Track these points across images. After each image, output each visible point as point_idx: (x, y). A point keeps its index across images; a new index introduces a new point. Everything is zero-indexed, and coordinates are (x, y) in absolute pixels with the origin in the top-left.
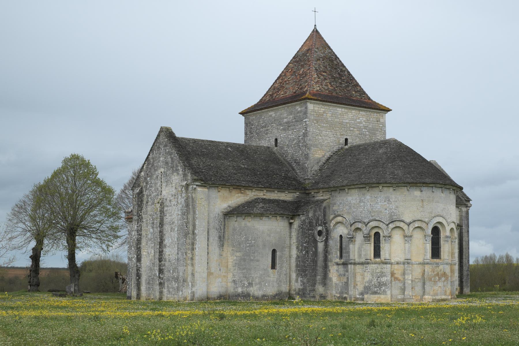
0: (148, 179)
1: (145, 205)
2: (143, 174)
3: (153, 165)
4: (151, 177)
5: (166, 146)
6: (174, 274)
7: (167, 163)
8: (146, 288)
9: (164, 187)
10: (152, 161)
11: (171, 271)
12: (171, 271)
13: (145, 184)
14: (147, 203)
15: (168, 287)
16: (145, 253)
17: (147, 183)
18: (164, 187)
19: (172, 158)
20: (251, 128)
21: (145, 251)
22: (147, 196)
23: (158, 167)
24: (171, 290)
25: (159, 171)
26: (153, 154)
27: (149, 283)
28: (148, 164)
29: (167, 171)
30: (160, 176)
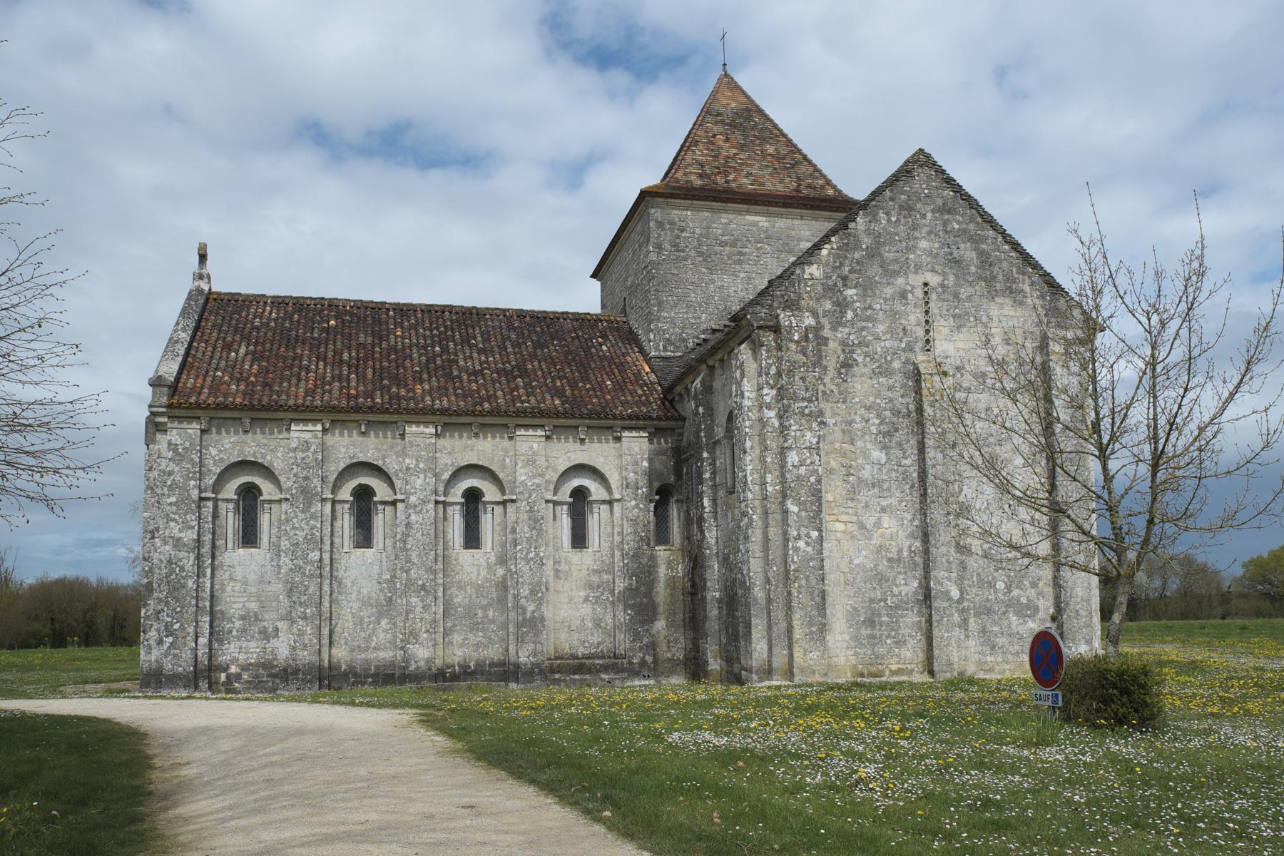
0: (851, 292)
1: (831, 373)
2: (813, 270)
3: (873, 254)
4: (868, 288)
5: (946, 209)
6: (1016, 592)
7: (957, 263)
8: (856, 638)
9: (947, 330)
10: (866, 241)
11: (1000, 585)
12: (1000, 585)
13: (828, 305)
14: (847, 365)
15: (984, 631)
16: (840, 527)
17: (842, 305)
18: (942, 328)
19: (981, 254)
20: (678, 237)
21: (844, 518)
22: (844, 343)
23: (904, 268)
24: (1001, 641)
25: (916, 280)
26: (875, 219)
27: (870, 622)
28: (845, 248)
29: (958, 285)
30: (919, 293)
